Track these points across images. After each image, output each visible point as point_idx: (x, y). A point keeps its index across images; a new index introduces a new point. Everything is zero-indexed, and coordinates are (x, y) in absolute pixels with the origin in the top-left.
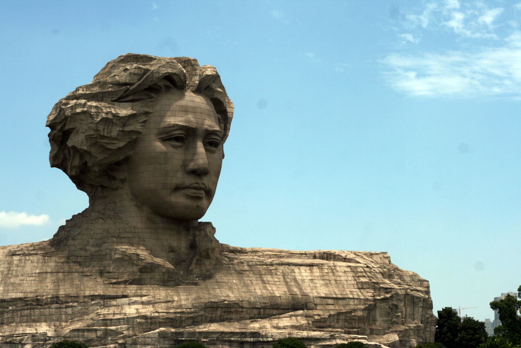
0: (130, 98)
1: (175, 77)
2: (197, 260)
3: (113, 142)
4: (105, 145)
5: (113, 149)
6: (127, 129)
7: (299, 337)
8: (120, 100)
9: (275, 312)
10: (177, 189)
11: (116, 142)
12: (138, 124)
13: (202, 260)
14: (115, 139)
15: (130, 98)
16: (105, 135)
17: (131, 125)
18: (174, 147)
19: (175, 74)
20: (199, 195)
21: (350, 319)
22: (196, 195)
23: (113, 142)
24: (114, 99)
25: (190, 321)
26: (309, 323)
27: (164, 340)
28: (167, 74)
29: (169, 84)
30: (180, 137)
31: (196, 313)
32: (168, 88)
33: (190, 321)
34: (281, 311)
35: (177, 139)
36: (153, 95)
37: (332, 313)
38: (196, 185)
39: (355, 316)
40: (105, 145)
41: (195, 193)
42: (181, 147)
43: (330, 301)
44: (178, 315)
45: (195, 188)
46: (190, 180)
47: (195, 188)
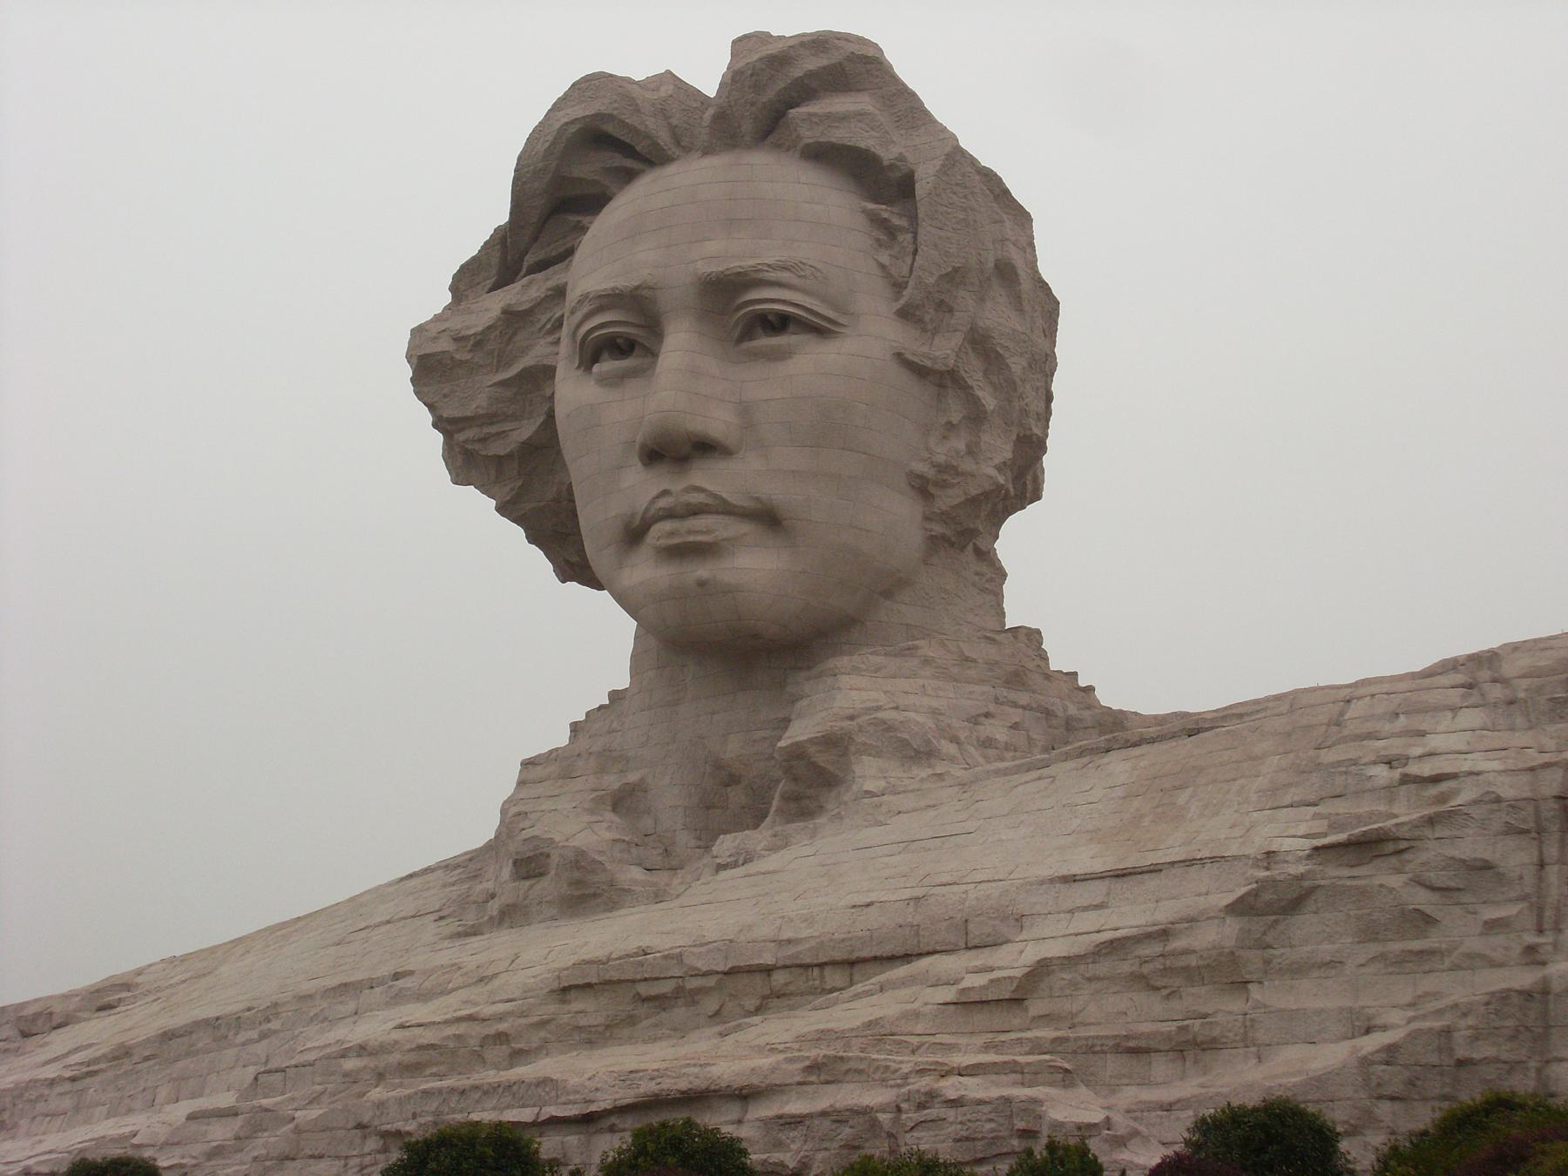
0: (529, 260)
1: (609, 128)
2: (787, 798)
3: (494, 429)
4: (477, 446)
5: (510, 456)
9: (834, 977)
11: (507, 427)
12: (542, 342)
13: (810, 792)
14: (491, 418)
15: (529, 260)
16: (457, 414)
17: (524, 351)
18: (604, 381)
19: (599, 116)
20: (691, 538)
21: (1166, 971)
22: (676, 541)
23: (494, 429)
24: (489, 283)
27: (365, 1137)
28: (573, 129)
29: (618, 160)
30: (619, 335)
31: (523, 1015)
32: (629, 176)
35: (620, 347)
36: (585, 220)
38: (664, 503)
40: (477, 446)
41: (672, 534)
45: (670, 514)
47: (670, 514)
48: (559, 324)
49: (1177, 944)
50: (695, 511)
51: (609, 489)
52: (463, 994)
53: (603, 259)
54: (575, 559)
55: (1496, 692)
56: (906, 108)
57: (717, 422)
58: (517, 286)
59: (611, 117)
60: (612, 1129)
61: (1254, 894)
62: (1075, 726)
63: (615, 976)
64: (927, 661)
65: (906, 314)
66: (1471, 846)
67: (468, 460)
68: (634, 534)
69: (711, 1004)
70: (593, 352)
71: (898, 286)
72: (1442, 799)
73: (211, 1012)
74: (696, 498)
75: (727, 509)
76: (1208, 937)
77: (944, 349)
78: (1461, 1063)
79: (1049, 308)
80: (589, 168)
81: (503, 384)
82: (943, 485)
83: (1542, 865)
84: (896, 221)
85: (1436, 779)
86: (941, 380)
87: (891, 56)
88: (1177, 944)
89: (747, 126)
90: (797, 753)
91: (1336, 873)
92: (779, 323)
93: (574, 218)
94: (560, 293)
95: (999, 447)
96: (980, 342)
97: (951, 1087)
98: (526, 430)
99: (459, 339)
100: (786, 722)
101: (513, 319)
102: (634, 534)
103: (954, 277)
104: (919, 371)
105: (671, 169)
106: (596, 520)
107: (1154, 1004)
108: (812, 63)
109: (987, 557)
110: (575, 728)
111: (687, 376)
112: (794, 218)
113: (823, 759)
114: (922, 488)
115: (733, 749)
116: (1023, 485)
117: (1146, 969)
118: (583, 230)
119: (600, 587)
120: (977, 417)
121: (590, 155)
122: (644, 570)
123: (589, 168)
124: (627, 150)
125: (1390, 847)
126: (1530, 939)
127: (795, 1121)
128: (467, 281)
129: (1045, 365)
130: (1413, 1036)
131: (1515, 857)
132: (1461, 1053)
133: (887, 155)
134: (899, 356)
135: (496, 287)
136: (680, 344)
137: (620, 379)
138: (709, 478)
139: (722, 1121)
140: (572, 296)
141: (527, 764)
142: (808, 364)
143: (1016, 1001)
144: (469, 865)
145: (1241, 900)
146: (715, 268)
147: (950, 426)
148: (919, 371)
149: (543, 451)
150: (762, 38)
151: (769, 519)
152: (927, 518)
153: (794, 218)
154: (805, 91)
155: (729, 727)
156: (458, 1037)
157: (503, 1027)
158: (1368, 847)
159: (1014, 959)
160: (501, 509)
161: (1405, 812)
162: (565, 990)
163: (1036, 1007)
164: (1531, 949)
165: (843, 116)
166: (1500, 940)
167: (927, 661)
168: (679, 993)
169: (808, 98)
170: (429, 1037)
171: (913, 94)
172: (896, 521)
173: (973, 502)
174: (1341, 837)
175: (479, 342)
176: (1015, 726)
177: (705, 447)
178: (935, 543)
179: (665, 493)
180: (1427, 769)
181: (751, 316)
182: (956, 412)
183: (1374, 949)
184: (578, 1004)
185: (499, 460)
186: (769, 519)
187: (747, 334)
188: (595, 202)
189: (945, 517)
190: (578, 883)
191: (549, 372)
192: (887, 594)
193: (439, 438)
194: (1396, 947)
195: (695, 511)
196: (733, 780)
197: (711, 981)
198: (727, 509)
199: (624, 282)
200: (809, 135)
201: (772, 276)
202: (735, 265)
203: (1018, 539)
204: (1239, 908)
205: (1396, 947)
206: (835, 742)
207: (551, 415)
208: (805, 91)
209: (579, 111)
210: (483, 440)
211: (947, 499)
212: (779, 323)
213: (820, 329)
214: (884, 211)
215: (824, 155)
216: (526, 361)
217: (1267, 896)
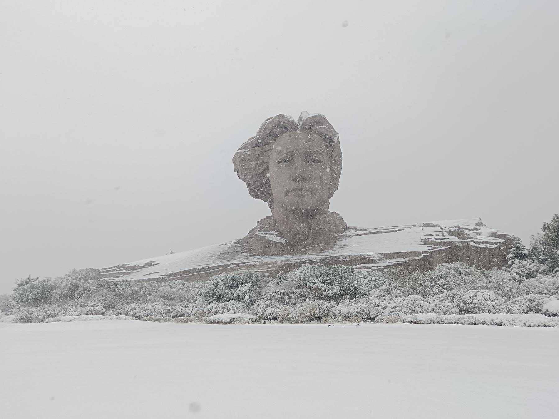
10: (287, 193)
32: (283, 132)
35: (286, 161)
46: (294, 185)
50: (302, 190)
86: (333, 171)
92: (314, 160)
101: (262, 153)
121: (278, 128)
124: (286, 129)
138: (306, 185)
151: (312, 192)
186: (312, 192)
195: (302, 190)
212: (314, 160)
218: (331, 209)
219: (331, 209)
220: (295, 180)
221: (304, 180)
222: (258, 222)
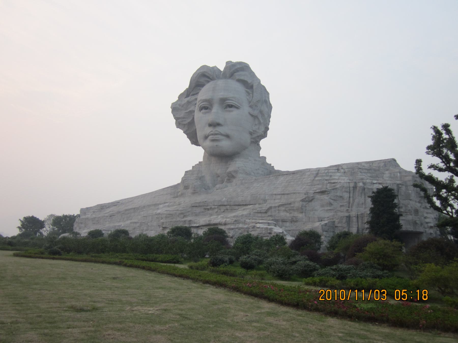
0: (191, 94)
2: (227, 180)
6: (188, 111)
7: (214, 222)
8: (187, 96)
9: (237, 207)
14: (184, 118)
15: (191, 94)
16: (178, 117)
18: (203, 113)
19: (205, 72)
21: (290, 210)
25: (182, 216)
26: (250, 214)
32: (208, 82)
33: (182, 216)
34: (242, 206)
35: (206, 108)
37: (273, 205)
38: (212, 133)
39: (294, 207)
42: (208, 112)
43: (279, 197)
44: (175, 212)
45: (212, 134)
46: (208, 130)
47: (212, 134)
48: (196, 104)
49: (292, 205)
50: (216, 134)
51: (202, 130)
52: (176, 206)
53: (204, 94)
54: (195, 141)
55: (342, 171)
56: (252, 74)
57: (221, 121)
58: (189, 98)
59: (206, 72)
60: (201, 229)
61: (305, 198)
62: (270, 172)
63: (201, 205)
64: (250, 160)
65: (251, 107)
66: (339, 194)
67: (179, 125)
68: (206, 137)
69: (216, 210)
70: (201, 109)
71: (250, 102)
72: (334, 186)
73: (134, 207)
74: (217, 132)
75: (221, 134)
76: (297, 205)
77: (256, 113)
78: (336, 227)
79: (270, 107)
80: (203, 80)
81: (186, 113)
82: (254, 133)
83: (350, 197)
84: (250, 92)
85: (334, 183)
86: (254, 117)
87: (250, 66)
88: (292, 205)
89: (228, 75)
90: (230, 173)
91: (318, 196)
92: (231, 106)
93: (199, 88)
94: (196, 99)
95: (263, 129)
96: (261, 112)
97: (258, 225)
98: (189, 120)
99: (180, 105)
100: (228, 168)
101: (189, 102)
102: (206, 137)
103: (258, 101)
104: (252, 116)
105: (215, 81)
106: (200, 135)
107: (288, 215)
108: (238, 66)
109: (258, 145)
110: (193, 167)
111: (216, 113)
112: (234, 91)
113: (234, 174)
114: (251, 134)
115: (219, 172)
116: (264, 135)
117: (287, 209)
118: (201, 90)
119: (200, 146)
120: (260, 123)
121: (203, 77)
122: (208, 143)
123: (203, 80)
124: (208, 77)
125: (327, 193)
126: (348, 208)
127: (233, 229)
128: (181, 96)
129: (269, 116)
130: (329, 222)
131: (346, 195)
132: (336, 225)
133: (249, 81)
134: (249, 113)
135: (185, 98)
136: (216, 108)
137: (205, 113)
138: (219, 129)
139: (220, 227)
140: (198, 100)
141: (186, 172)
142: (234, 113)
143: (266, 213)
144: (175, 187)
145: (303, 199)
146: (221, 97)
147: (256, 124)
148: (252, 116)
149: (192, 123)
150: (231, 62)
151: (228, 136)
152: (251, 138)
153: (234, 91)
154: (237, 71)
155: (219, 168)
156: (176, 213)
157: (182, 212)
158: (323, 192)
159: (265, 207)
160: (184, 132)
161: (329, 187)
162: (193, 207)
163: (269, 213)
164: (347, 210)
165: (242, 75)
166: (342, 208)
167: (250, 160)
168: (211, 208)
169: (238, 72)
170: (171, 213)
171: (253, 73)
172: (247, 139)
173: (258, 136)
174: (319, 191)
175: (183, 106)
176: (262, 171)
177: (218, 125)
178: (252, 142)
179: (212, 131)
180: (332, 181)
181: (227, 105)
182: (257, 122)
183: (323, 208)
184: (195, 209)
185: (184, 125)
186: (228, 136)
187: (226, 108)
188: (203, 85)
189: (254, 138)
190: (195, 190)
191: (194, 111)
192: (244, 150)
193: (175, 120)
194: (326, 208)
195: (216, 134)
196: (219, 176)
197: (216, 207)
198: (221, 134)
199: (208, 98)
200: (237, 77)
201: (231, 99)
202: (225, 97)
203: (262, 143)
204: (303, 201)
205: (326, 208)
206: (236, 172)
207: (193, 118)
208: (237, 71)
209: (201, 71)
210: (182, 121)
211: (254, 136)
212: (231, 106)
213: (237, 108)
214: (248, 90)
215: (239, 81)
216: (190, 109)
217: (307, 199)
218: (262, 154)
219: (262, 154)
220: (210, 125)
221: (218, 125)
222: (193, 167)
